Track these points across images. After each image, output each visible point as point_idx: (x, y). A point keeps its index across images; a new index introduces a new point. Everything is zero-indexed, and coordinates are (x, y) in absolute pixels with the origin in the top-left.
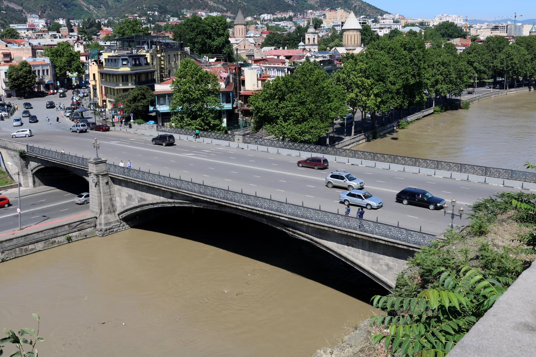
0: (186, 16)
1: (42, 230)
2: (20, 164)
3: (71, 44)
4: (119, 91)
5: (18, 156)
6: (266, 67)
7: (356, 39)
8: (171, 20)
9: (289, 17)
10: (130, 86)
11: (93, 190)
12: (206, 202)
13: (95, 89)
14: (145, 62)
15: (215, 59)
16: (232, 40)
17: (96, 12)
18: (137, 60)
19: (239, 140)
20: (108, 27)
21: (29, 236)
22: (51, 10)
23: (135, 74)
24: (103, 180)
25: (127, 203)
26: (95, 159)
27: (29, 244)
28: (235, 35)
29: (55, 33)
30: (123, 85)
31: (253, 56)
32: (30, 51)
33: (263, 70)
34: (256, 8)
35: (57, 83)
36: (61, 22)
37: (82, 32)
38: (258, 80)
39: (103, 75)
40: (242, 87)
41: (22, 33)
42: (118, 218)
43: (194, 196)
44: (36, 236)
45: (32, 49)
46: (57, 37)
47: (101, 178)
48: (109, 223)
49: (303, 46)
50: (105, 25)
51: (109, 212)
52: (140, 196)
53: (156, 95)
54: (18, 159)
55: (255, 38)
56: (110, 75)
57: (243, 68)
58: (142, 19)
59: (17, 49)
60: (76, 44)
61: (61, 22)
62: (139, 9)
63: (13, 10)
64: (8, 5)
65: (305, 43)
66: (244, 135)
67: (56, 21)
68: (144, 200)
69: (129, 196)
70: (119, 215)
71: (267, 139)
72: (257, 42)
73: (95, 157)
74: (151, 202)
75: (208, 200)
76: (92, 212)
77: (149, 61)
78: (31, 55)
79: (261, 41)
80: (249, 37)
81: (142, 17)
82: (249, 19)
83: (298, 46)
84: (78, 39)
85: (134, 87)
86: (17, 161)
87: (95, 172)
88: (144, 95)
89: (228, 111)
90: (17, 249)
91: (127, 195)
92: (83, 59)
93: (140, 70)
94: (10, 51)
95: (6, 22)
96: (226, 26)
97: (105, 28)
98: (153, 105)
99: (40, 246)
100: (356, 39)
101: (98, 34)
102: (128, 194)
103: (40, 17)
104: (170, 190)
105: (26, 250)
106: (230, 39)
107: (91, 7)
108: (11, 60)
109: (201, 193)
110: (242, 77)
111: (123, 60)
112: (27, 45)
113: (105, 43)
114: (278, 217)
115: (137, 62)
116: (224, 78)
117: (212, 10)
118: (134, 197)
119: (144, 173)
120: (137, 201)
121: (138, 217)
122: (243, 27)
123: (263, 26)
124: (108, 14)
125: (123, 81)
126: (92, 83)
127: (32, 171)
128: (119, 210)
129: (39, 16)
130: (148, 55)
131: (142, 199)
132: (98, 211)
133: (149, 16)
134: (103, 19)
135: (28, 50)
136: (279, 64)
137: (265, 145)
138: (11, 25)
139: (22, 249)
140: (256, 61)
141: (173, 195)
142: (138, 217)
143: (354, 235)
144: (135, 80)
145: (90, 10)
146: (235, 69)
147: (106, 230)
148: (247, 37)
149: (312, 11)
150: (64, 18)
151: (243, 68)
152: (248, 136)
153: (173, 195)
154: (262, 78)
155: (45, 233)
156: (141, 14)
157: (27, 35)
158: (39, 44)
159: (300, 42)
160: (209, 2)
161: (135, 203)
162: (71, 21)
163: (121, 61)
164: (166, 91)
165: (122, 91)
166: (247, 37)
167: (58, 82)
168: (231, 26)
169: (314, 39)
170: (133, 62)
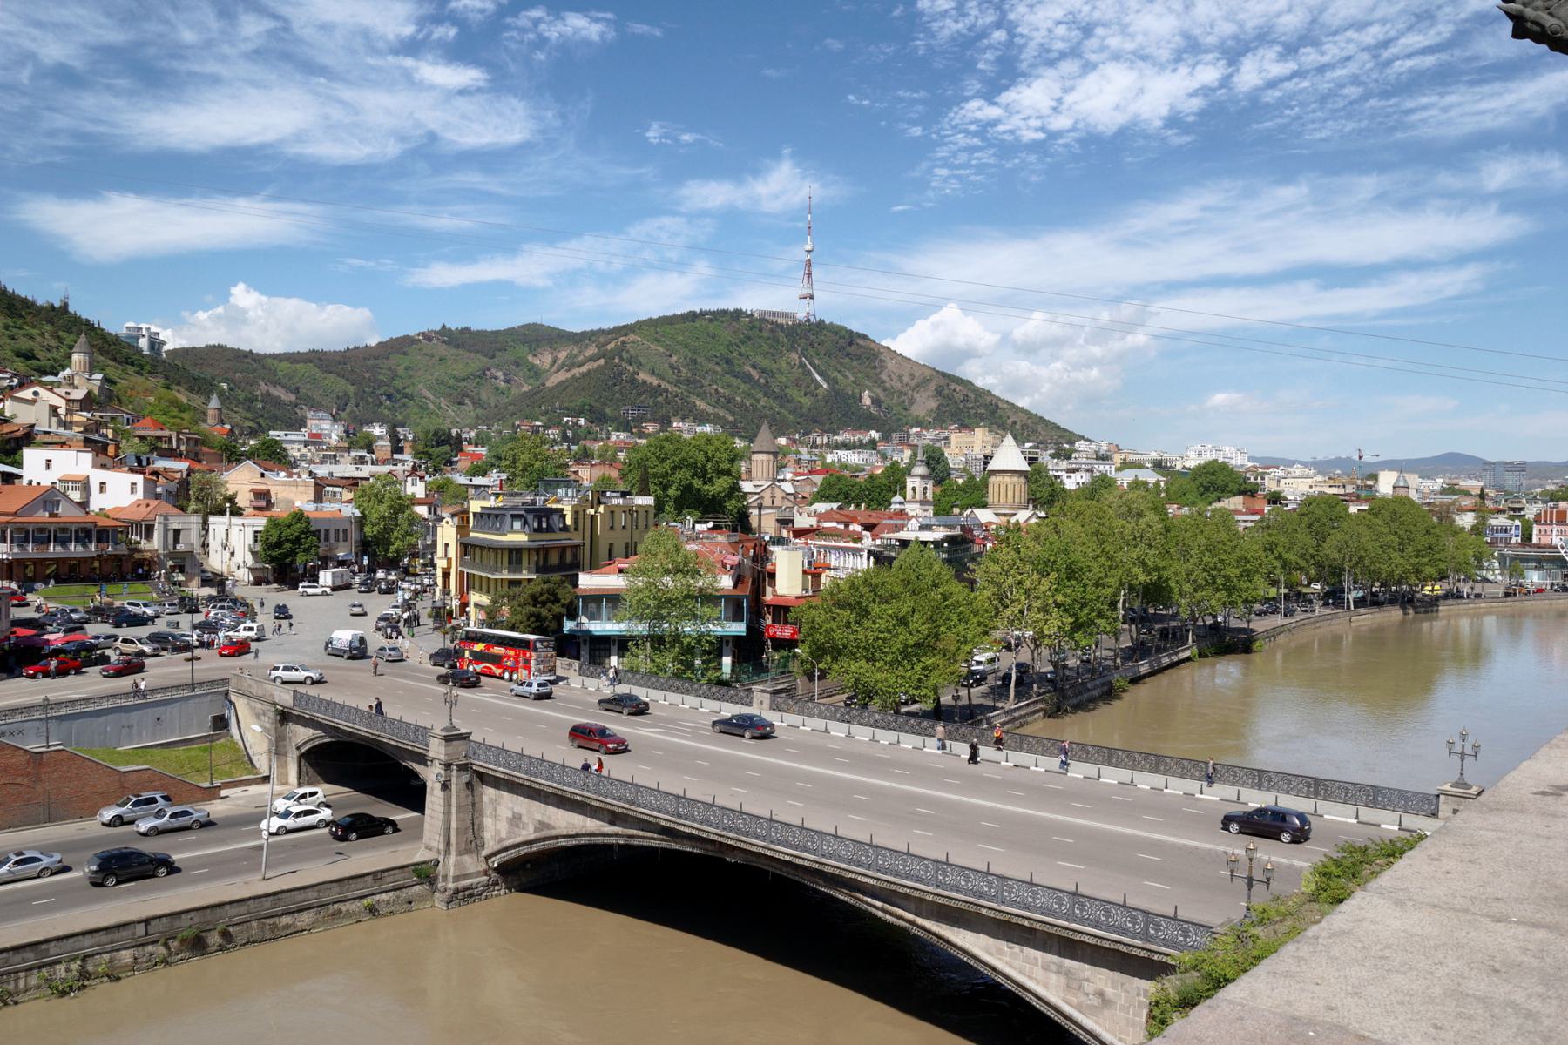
0: (647, 431)
1: (315, 882)
2: (273, 732)
3: (400, 478)
4: (499, 584)
5: (272, 715)
6: (820, 547)
7: (1017, 493)
8: (614, 438)
9: (870, 441)
10: (525, 575)
11: (434, 799)
12: (690, 837)
13: (446, 575)
14: (561, 526)
15: (711, 524)
16: (746, 486)
17: (453, 414)
18: (544, 520)
19: (761, 703)
20: (476, 446)
21: (284, 895)
22: (357, 406)
23: (537, 550)
24: (458, 777)
25: (509, 832)
26: (444, 730)
27: (282, 915)
28: (754, 475)
29: (363, 453)
30: (509, 572)
31: (792, 521)
32: (312, 490)
33: (813, 553)
34: (799, 420)
35: (362, 559)
36: (377, 430)
37: (423, 453)
38: (805, 572)
39: (467, 548)
40: (769, 589)
41: (294, 451)
42: (484, 866)
43: (663, 823)
44: (300, 896)
45: (316, 484)
46: (367, 462)
47: (455, 773)
48: (464, 875)
49: (901, 503)
50: (470, 443)
51: (468, 851)
52: (538, 817)
53: (581, 596)
54: (269, 720)
55: (795, 483)
56: (481, 547)
57: (771, 548)
58: (550, 432)
59: (284, 484)
60: (409, 479)
61: (377, 430)
62: (546, 412)
63: (278, 402)
64: (268, 391)
65: (905, 498)
66: (775, 693)
67: (366, 429)
68: (548, 826)
69: (514, 817)
70: (487, 858)
71: (824, 704)
72: (799, 490)
73: (446, 724)
74: (565, 833)
75: (695, 832)
76: (429, 848)
77: (569, 521)
78: (312, 497)
79: (808, 491)
80: (783, 480)
81: (550, 428)
82: (782, 441)
83: (890, 505)
84: (415, 469)
85: (534, 577)
86: (268, 726)
87: (442, 757)
88: (554, 595)
89: (737, 639)
90: (255, 924)
91: (510, 815)
92: (422, 511)
93: (545, 540)
94: (269, 487)
95: (260, 425)
96: (735, 457)
97: (471, 449)
98: (573, 615)
99: (305, 918)
100: (1017, 493)
101: (456, 459)
102: (514, 813)
103: (335, 419)
104: (609, 807)
105: (275, 927)
106: (741, 483)
107: (443, 403)
108: (270, 505)
109: (680, 816)
110: (769, 566)
111: (514, 517)
112: (305, 476)
113: (471, 480)
114: (853, 876)
115: (544, 525)
116: (731, 568)
117: (701, 419)
118: (525, 819)
119: (553, 765)
120: (531, 828)
121: (529, 866)
122: (771, 457)
123: (814, 458)
124: (477, 417)
125: (510, 563)
126: (441, 563)
127: (298, 748)
128: (491, 845)
129: (333, 416)
130: (568, 511)
131: (543, 825)
132: (442, 847)
133: (566, 427)
134: (467, 429)
135: (306, 485)
136: (848, 542)
137: (820, 716)
138: (271, 432)
139: (264, 924)
140: (799, 533)
141: (614, 818)
142: (529, 866)
143: (1026, 923)
144: (537, 563)
145: (440, 408)
146: (754, 548)
147: (457, 891)
148: (779, 481)
149: (918, 429)
150: (382, 423)
151: (771, 548)
152: (784, 695)
153: (614, 818)
154: (813, 572)
155: (319, 891)
156: (549, 420)
157: (303, 456)
158: (331, 474)
159: (895, 493)
160: (698, 403)
161: (528, 833)
162: (399, 429)
163: (508, 519)
164: (604, 589)
165: (506, 585)
166: (779, 481)
167: (366, 558)
168: (746, 455)
169: (925, 489)
170: (536, 525)
